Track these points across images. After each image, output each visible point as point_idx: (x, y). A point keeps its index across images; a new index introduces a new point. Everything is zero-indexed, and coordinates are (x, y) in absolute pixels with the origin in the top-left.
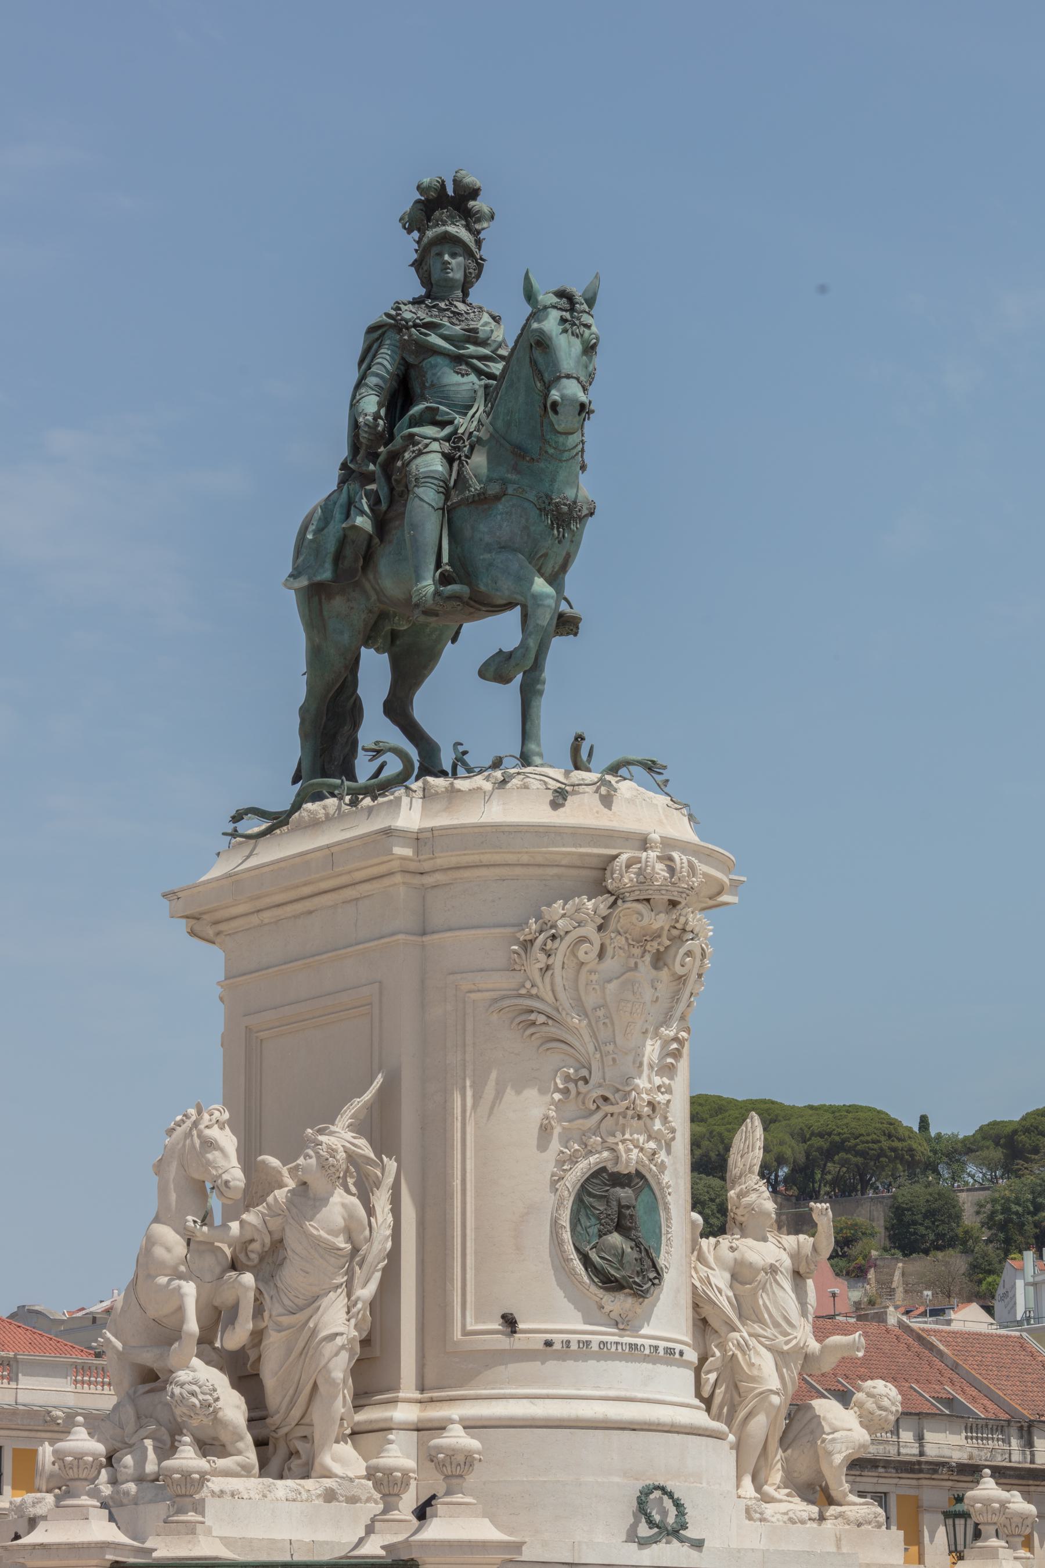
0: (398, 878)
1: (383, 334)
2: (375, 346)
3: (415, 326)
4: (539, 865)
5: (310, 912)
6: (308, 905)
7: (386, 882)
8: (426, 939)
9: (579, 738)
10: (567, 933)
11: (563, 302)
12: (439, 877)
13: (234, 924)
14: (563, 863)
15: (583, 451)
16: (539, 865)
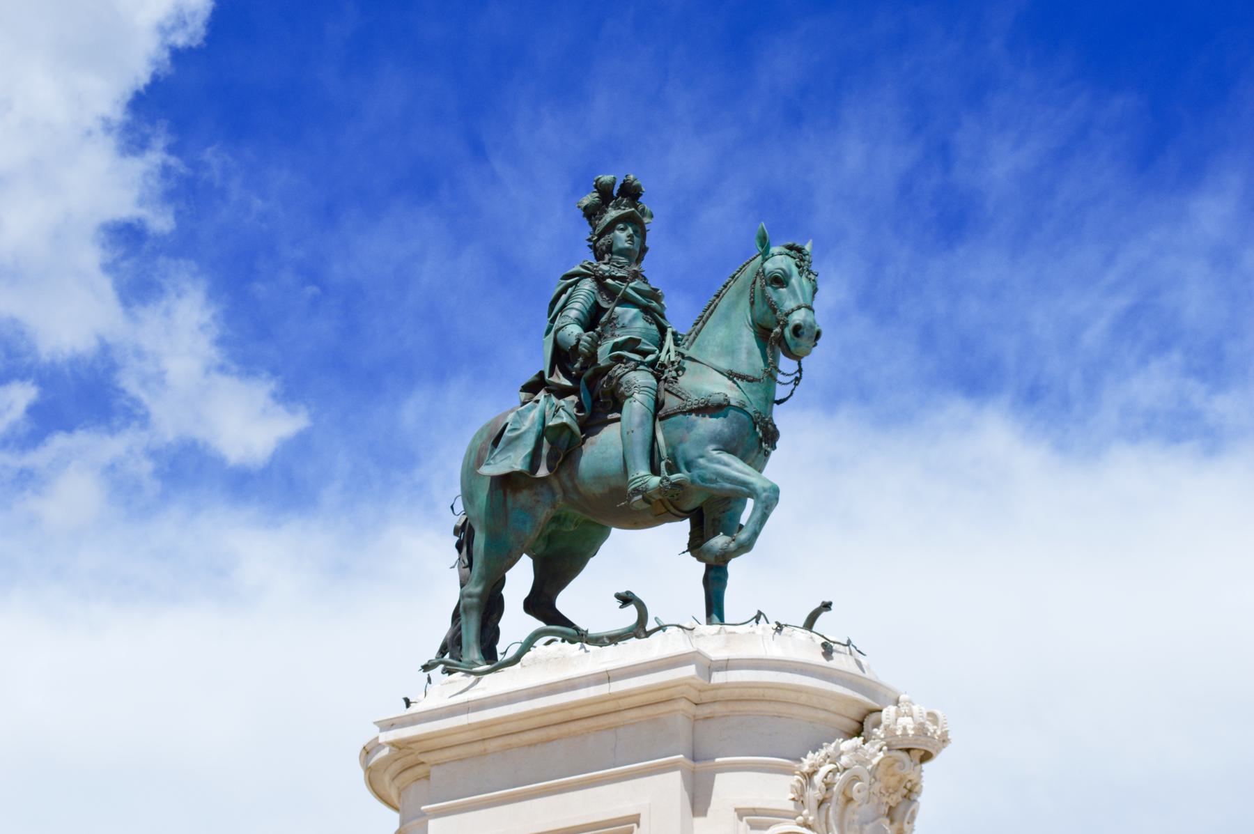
0: (682, 705)
1: (576, 283)
2: (570, 290)
3: (614, 278)
4: (814, 708)
5: (550, 740)
6: (553, 732)
7: (663, 708)
8: (698, 765)
9: (827, 606)
10: (845, 769)
11: (793, 253)
12: (717, 708)
13: (448, 754)
14: (833, 708)
15: (798, 379)
16: (814, 708)
